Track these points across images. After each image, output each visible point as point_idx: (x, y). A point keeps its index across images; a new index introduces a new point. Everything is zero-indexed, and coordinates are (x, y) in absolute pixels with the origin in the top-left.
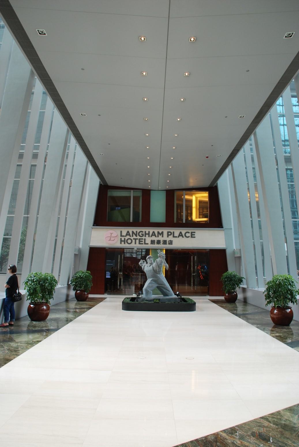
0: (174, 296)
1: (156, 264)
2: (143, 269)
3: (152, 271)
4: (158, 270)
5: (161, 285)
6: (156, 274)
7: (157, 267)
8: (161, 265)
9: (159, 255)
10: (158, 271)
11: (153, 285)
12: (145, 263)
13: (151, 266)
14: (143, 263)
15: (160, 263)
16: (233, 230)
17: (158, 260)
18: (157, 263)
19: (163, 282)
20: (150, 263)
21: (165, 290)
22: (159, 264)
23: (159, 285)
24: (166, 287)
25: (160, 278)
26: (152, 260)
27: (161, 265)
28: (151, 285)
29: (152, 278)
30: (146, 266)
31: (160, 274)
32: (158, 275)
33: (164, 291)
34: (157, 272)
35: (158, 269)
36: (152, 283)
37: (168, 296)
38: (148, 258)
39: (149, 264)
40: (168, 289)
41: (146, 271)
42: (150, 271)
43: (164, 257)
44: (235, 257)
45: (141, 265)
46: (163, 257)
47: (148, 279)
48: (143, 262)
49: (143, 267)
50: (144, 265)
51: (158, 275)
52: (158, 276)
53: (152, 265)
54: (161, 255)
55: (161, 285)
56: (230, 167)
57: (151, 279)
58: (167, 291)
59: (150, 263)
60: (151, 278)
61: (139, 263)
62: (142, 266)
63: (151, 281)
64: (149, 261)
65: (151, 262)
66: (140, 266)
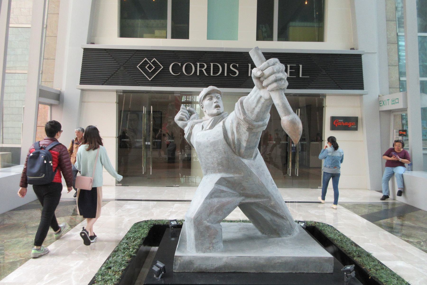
1: (242, 117)
2: (186, 136)
3: (222, 146)
4: (248, 142)
5: (256, 196)
6: (236, 157)
7: (244, 129)
8: (260, 123)
9: (259, 74)
10: (244, 144)
11: (225, 200)
12: (194, 118)
13: (219, 127)
14: (189, 119)
15: (257, 110)
18: (244, 113)
19: (262, 186)
20: (212, 115)
21: (267, 217)
22: (252, 117)
23: (248, 200)
24: (273, 207)
25: (251, 172)
26: (221, 104)
27: (262, 119)
28: (215, 200)
29: (220, 172)
30: (197, 128)
31: (249, 156)
32: (246, 161)
33: (265, 221)
34: (243, 150)
36: (222, 191)
39: (208, 120)
40: (278, 212)
41: (199, 144)
42: (214, 144)
43: (281, 79)
44: (380, 111)
45: (180, 124)
46: (276, 81)
47: (205, 175)
48: (187, 115)
49: (186, 130)
50: (190, 123)
52: (245, 165)
53: (221, 123)
54: (267, 72)
55: (256, 196)
57: (217, 177)
59: (212, 115)
60: (215, 172)
61: (177, 117)
62: (185, 125)
63: (219, 182)
64: (210, 105)
65: (215, 111)
66: (179, 128)
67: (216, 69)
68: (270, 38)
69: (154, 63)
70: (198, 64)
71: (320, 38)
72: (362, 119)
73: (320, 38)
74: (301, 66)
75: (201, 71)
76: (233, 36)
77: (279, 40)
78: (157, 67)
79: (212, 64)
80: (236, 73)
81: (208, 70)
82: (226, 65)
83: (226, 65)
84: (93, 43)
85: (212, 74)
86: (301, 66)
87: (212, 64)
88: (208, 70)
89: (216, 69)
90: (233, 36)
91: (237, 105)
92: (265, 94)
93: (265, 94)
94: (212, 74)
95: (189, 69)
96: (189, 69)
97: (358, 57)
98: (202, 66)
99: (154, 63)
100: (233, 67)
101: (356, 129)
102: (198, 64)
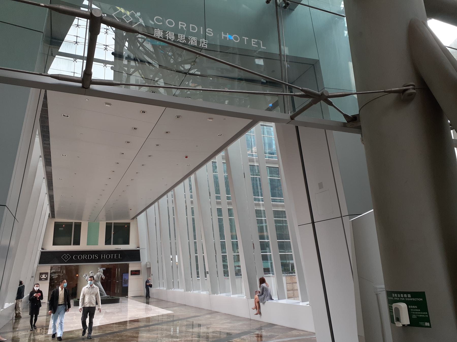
0: (106, 295)
7: (97, 278)
16: (146, 250)
17: (98, 273)
31: (98, 282)
32: (97, 283)
35: (97, 279)
37: (103, 296)
38: (91, 272)
51: (97, 283)
56: (145, 212)
58: (103, 293)
67: (90, 257)
68: (110, 244)
69: (68, 256)
70: (84, 255)
71: (128, 243)
72: (141, 271)
73: (128, 243)
74: (119, 254)
75: (85, 258)
76: (96, 244)
77: (113, 245)
78: (69, 257)
79: (89, 255)
80: (97, 258)
81: (87, 257)
82: (93, 255)
83: (93, 255)
84: (43, 250)
85: (88, 259)
86: (119, 254)
87: (89, 255)
88: (87, 257)
89: (90, 257)
90: (96, 244)
91: (96, 274)
92: (100, 273)
93: (100, 273)
94: (88, 259)
95: (80, 257)
96: (80, 257)
97: (139, 250)
98: (85, 256)
99: (68, 256)
100: (96, 256)
101: (139, 274)
102: (84, 255)
